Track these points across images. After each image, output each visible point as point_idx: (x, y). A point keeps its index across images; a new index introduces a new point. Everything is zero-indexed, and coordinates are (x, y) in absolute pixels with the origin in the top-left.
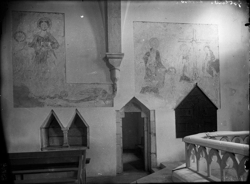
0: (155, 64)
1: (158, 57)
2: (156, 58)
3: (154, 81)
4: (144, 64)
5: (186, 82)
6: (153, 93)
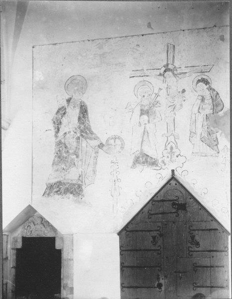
0: (75, 132)
1: (84, 117)
2: (79, 118)
3: (73, 169)
4: (54, 134)
6: (71, 196)
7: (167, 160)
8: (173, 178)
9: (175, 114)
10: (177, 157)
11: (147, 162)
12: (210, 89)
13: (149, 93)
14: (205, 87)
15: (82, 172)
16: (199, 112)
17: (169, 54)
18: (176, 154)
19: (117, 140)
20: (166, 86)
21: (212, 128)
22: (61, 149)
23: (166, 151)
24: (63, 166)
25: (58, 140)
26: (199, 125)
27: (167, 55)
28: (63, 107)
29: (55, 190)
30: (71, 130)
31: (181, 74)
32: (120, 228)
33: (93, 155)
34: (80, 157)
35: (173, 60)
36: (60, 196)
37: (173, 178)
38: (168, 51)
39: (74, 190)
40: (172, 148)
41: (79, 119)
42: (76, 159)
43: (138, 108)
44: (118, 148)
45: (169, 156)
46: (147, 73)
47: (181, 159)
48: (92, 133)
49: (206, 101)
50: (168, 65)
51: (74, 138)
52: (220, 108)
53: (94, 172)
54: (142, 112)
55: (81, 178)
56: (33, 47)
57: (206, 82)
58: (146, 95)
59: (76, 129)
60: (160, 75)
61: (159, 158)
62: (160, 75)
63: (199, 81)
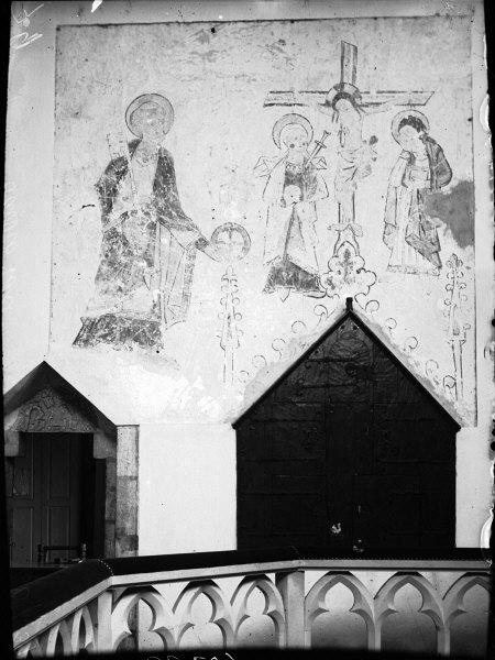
0: (147, 214)
1: (166, 181)
2: (156, 185)
3: (140, 291)
4: (100, 213)
5: (297, 297)
6: (135, 345)
7: (337, 279)
8: (349, 314)
9: (355, 185)
10: (358, 272)
11: (296, 280)
12: (427, 139)
13: (304, 140)
14: (416, 135)
15: (159, 296)
16: (403, 184)
18: (356, 267)
19: (235, 233)
21: (428, 218)
22: (114, 247)
24: (119, 283)
25: (108, 228)
26: (403, 209)
28: (121, 159)
29: (102, 332)
30: (138, 208)
32: (237, 414)
33: (185, 261)
34: (157, 267)
35: (354, 77)
36: (112, 345)
37: (349, 314)
38: (343, 57)
39: (142, 334)
40: (347, 254)
41: (155, 185)
42: (147, 270)
44: (237, 250)
45: (343, 271)
46: (301, 99)
47: (366, 278)
48: (182, 216)
51: (143, 224)
52: (444, 178)
53: (186, 297)
55: (156, 310)
56: (58, 29)
57: (418, 124)
58: (297, 144)
59: (148, 206)
60: (327, 104)
61: (320, 273)
62: (327, 104)
63: (404, 122)
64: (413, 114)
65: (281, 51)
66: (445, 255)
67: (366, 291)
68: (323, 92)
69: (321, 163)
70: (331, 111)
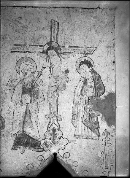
5: (29, 152)
7: (49, 142)
9: (58, 94)
12: (93, 71)
13: (32, 70)
14: (88, 69)
17: (52, 31)
18: (58, 136)
20: (49, 65)
21: (94, 112)
23: (49, 133)
26: (82, 108)
27: (51, 31)
31: (64, 53)
35: (57, 38)
40: (54, 130)
43: (20, 86)
45: (52, 138)
49: (88, 84)
50: (51, 42)
52: (101, 91)
54: (25, 91)
57: (89, 64)
58: (29, 73)
60: (43, 52)
61: (41, 140)
62: (43, 52)
63: (82, 63)
64: (86, 58)
65: (20, 23)
66: (101, 131)
67: (63, 148)
68: (42, 46)
69: (41, 83)
70: (46, 56)
